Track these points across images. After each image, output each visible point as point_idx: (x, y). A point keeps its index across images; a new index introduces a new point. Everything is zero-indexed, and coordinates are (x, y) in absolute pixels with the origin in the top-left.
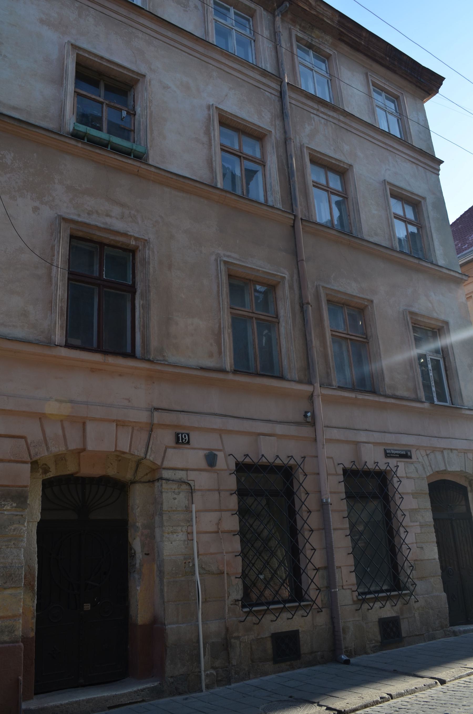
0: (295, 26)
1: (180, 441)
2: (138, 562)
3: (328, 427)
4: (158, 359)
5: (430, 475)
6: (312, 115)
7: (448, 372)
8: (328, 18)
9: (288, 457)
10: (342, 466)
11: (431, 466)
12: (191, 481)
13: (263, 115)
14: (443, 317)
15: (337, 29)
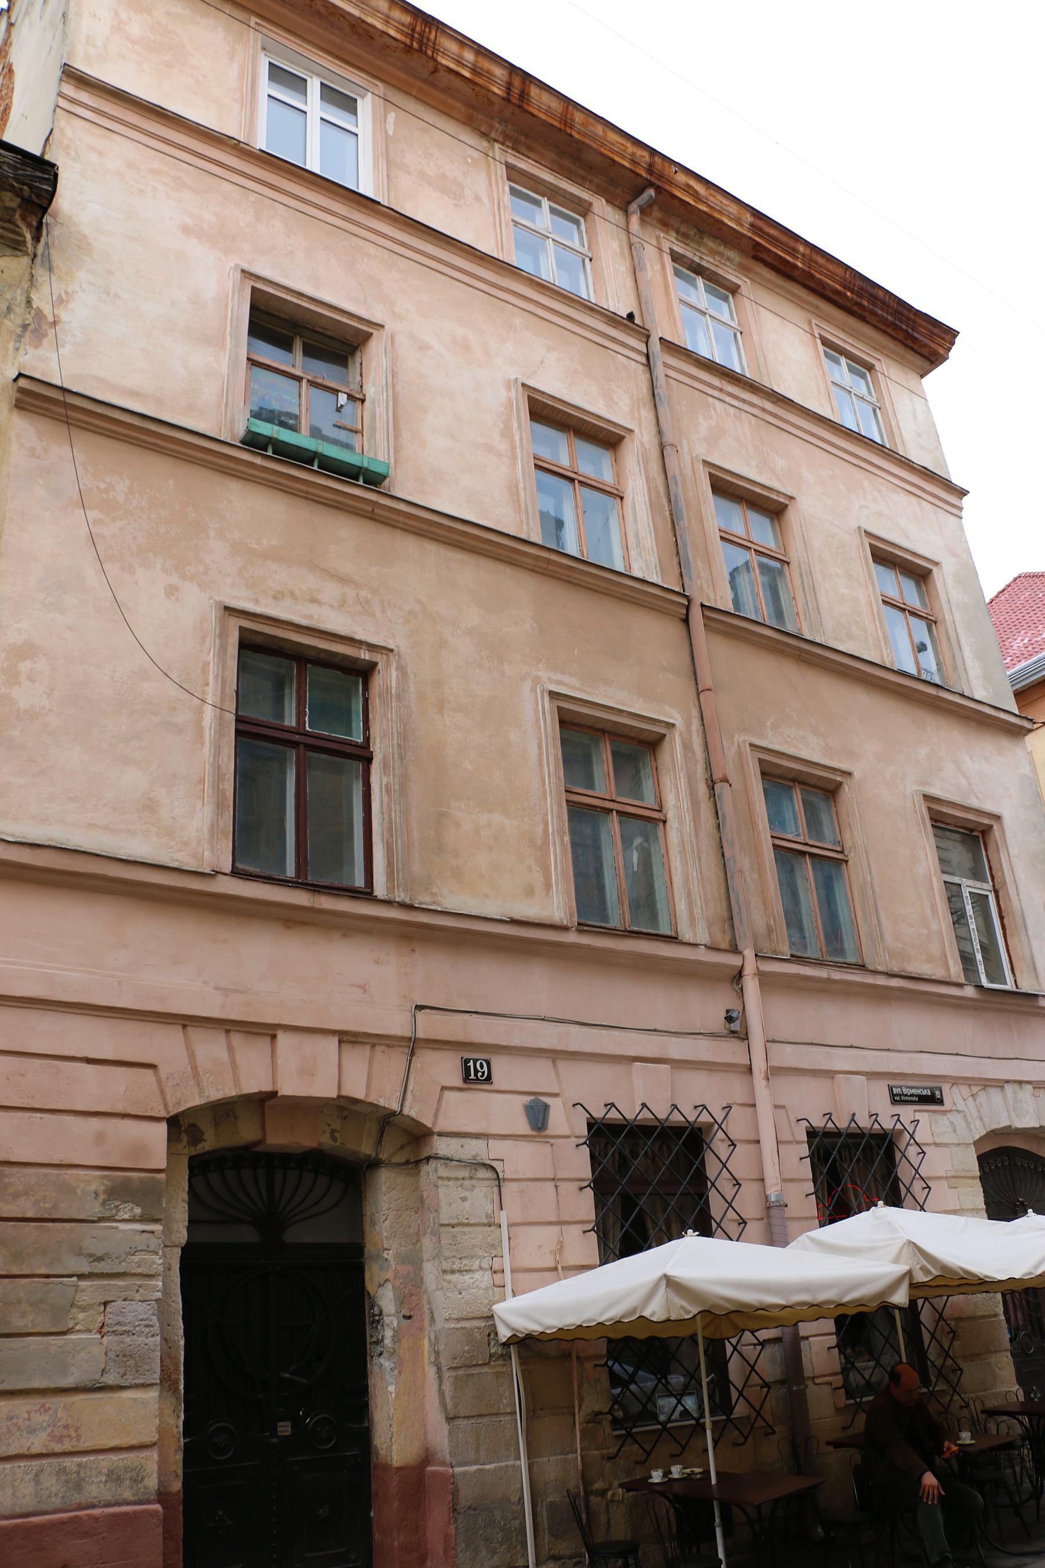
0: (667, 233)
1: (472, 1077)
2: (388, 1334)
3: (773, 1041)
4: (423, 900)
5: (981, 1139)
6: (710, 399)
7: (1005, 921)
8: (731, 219)
9: (696, 1107)
10: (805, 1124)
11: (981, 1119)
12: (497, 1162)
13: (616, 399)
14: (989, 807)
15: (750, 238)
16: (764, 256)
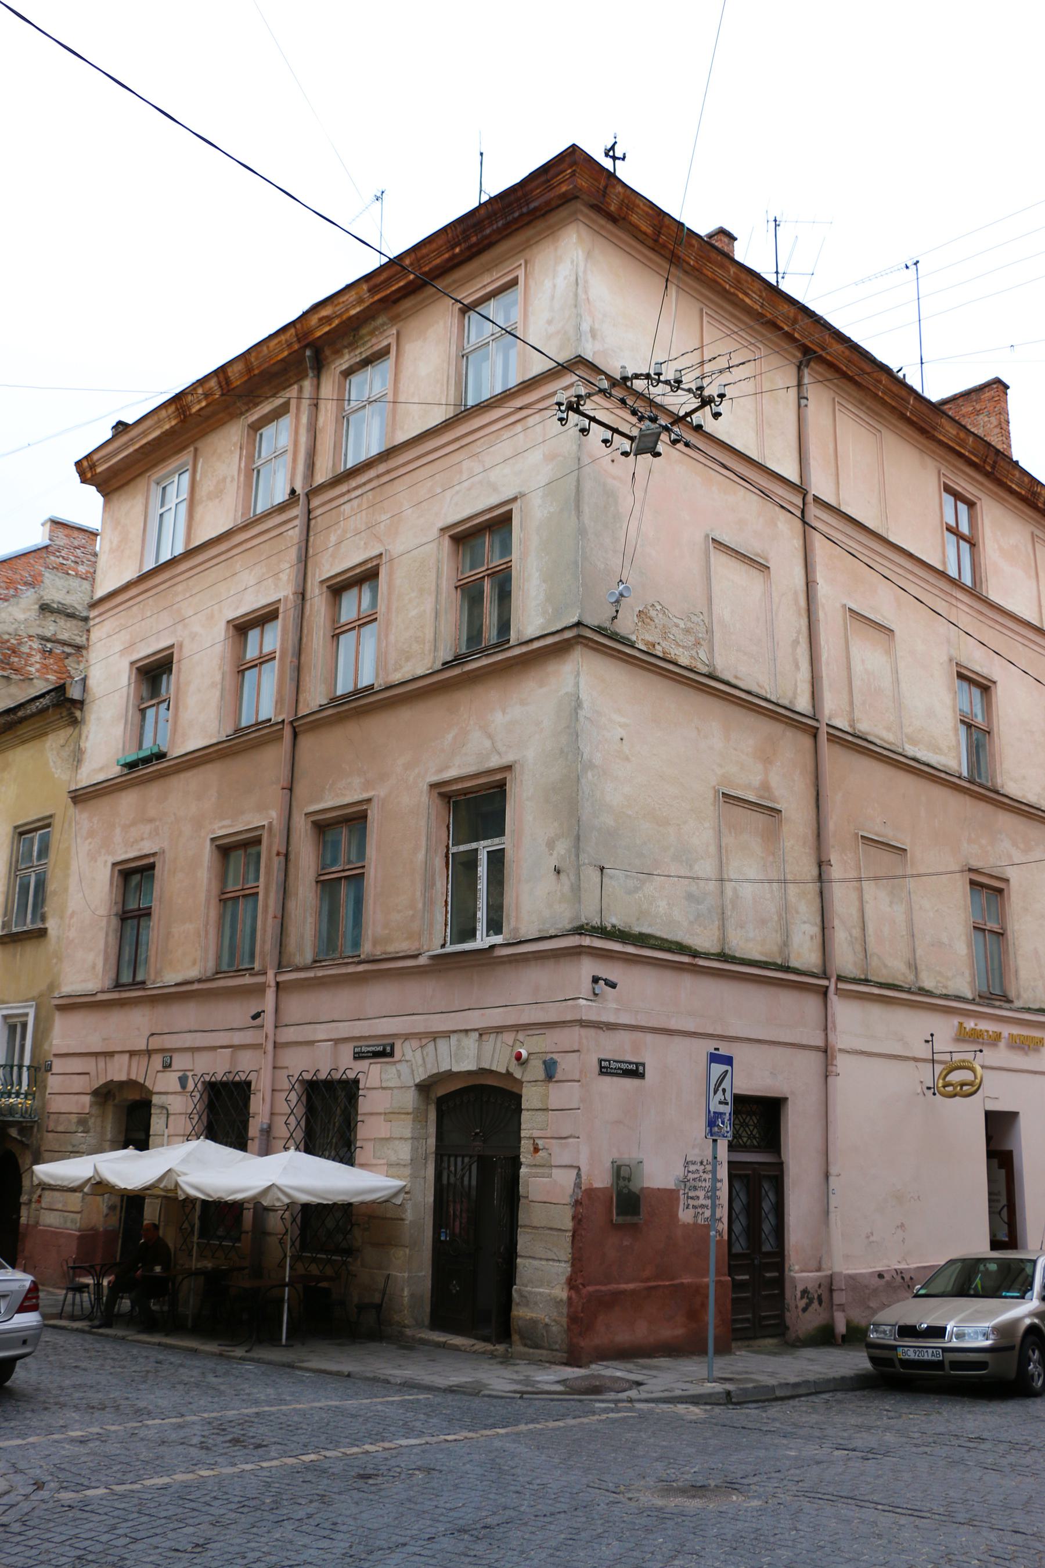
16: (394, 297)
